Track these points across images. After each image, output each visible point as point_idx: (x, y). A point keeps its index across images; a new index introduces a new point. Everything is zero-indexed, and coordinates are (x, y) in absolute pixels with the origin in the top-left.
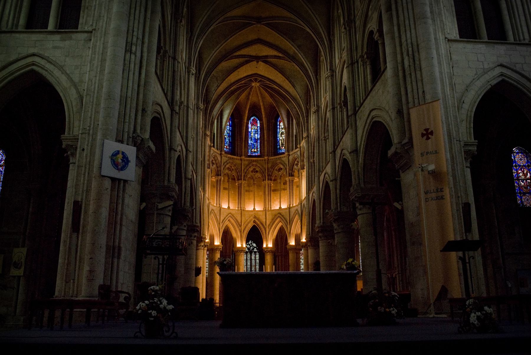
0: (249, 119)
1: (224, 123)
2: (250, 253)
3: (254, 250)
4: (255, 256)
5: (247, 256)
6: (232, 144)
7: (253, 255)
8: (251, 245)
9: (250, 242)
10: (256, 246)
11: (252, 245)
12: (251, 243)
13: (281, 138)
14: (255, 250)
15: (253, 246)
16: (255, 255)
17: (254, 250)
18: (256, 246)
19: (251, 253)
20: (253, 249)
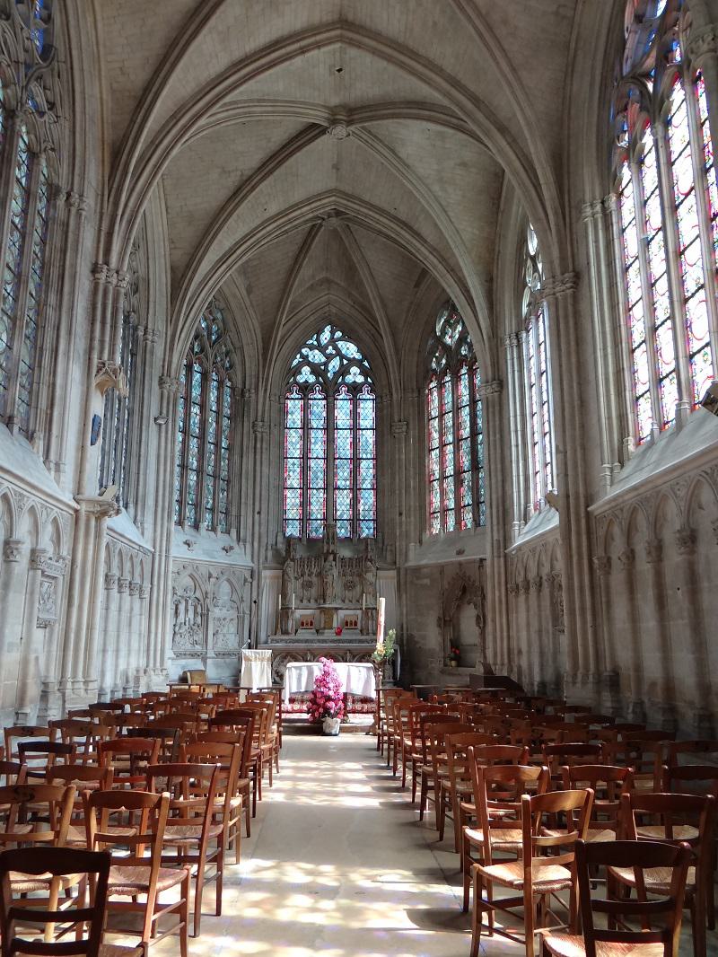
3: (349, 379)
4: (355, 406)
7: (339, 403)
8: (330, 350)
9: (326, 336)
10: (358, 356)
11: (336, 348)
12: (333, 341)
14: (355, 376)
15: (342, 357)
16: (355, 403)
17: (349, 379)
18: (358, 356)
19: (330, 391)
20: (343, 371)
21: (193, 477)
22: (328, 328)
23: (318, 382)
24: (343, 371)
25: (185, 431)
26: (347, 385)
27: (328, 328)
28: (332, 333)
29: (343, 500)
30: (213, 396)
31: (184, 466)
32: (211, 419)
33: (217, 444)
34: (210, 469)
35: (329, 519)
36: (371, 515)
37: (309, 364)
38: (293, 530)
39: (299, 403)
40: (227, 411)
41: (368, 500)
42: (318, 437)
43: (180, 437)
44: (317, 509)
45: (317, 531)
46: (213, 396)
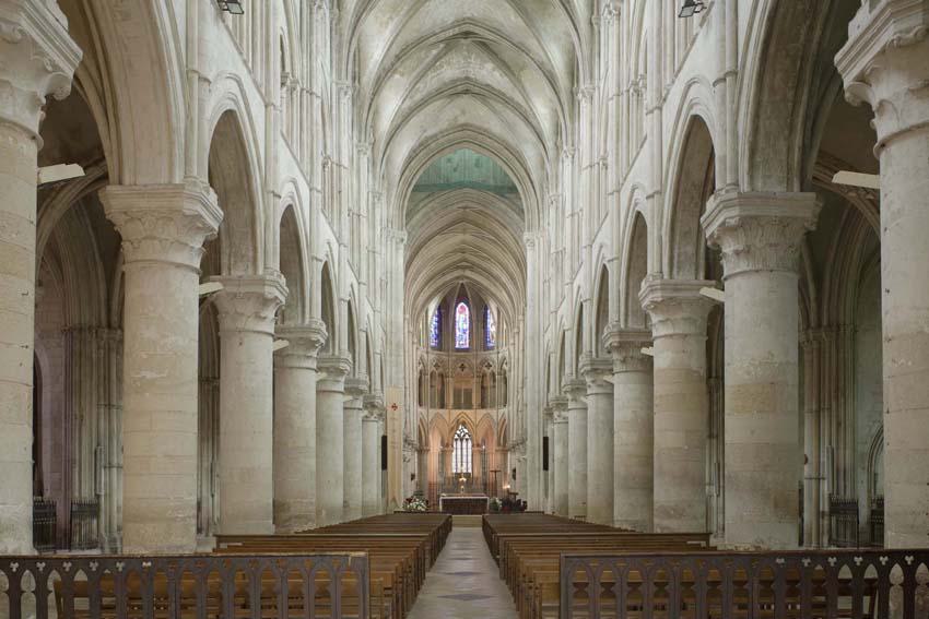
0: (456, 306)
1: (429, 319)
6: (439, 336)
13: (492, 329)
14: (467, 437)
19: (461, 440)
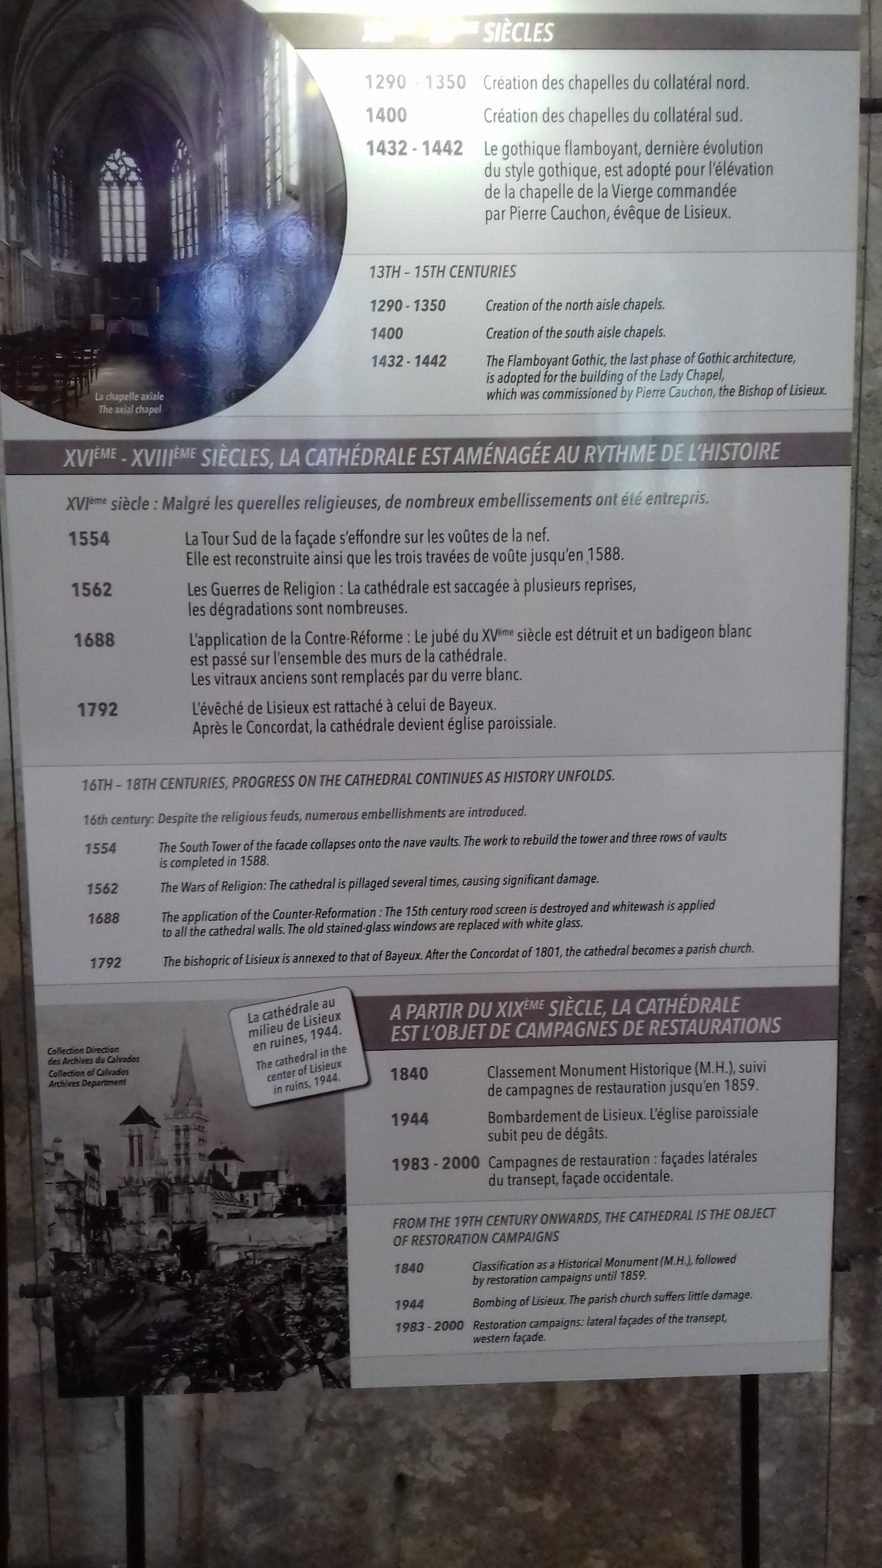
2: (118, 185)
5: (109, 195)
8: (120, 163)
9: (118, 153)
10: (135, 166)
12: (121, 158)
14: (133, 177)
15: (127, 166)
16: (134, 190)
19: (121, 183)
20: (127, 174)
21: (58, 231)
22: (118, 150)
23: (115, 180)
24: (127, 174)
25: (52, 207)
26: (130, 182)
27: (118, 150)
28: (121, 153)
29: (130, 242)
30: (64, 189)
31: (53, 225)
32: (64, 201)
33: (68, 214)
34: (65, 227)
35: (124, 255)
36: (144, 251)
37: (110, 170)
38: (106, 258)
39: (106, 192)
40: (71, 196)
41: (142, 244)
42: (116, 211)
43: (49, 210)
44: (118, 247)
45: (118, 259)
46: (64, 189)
